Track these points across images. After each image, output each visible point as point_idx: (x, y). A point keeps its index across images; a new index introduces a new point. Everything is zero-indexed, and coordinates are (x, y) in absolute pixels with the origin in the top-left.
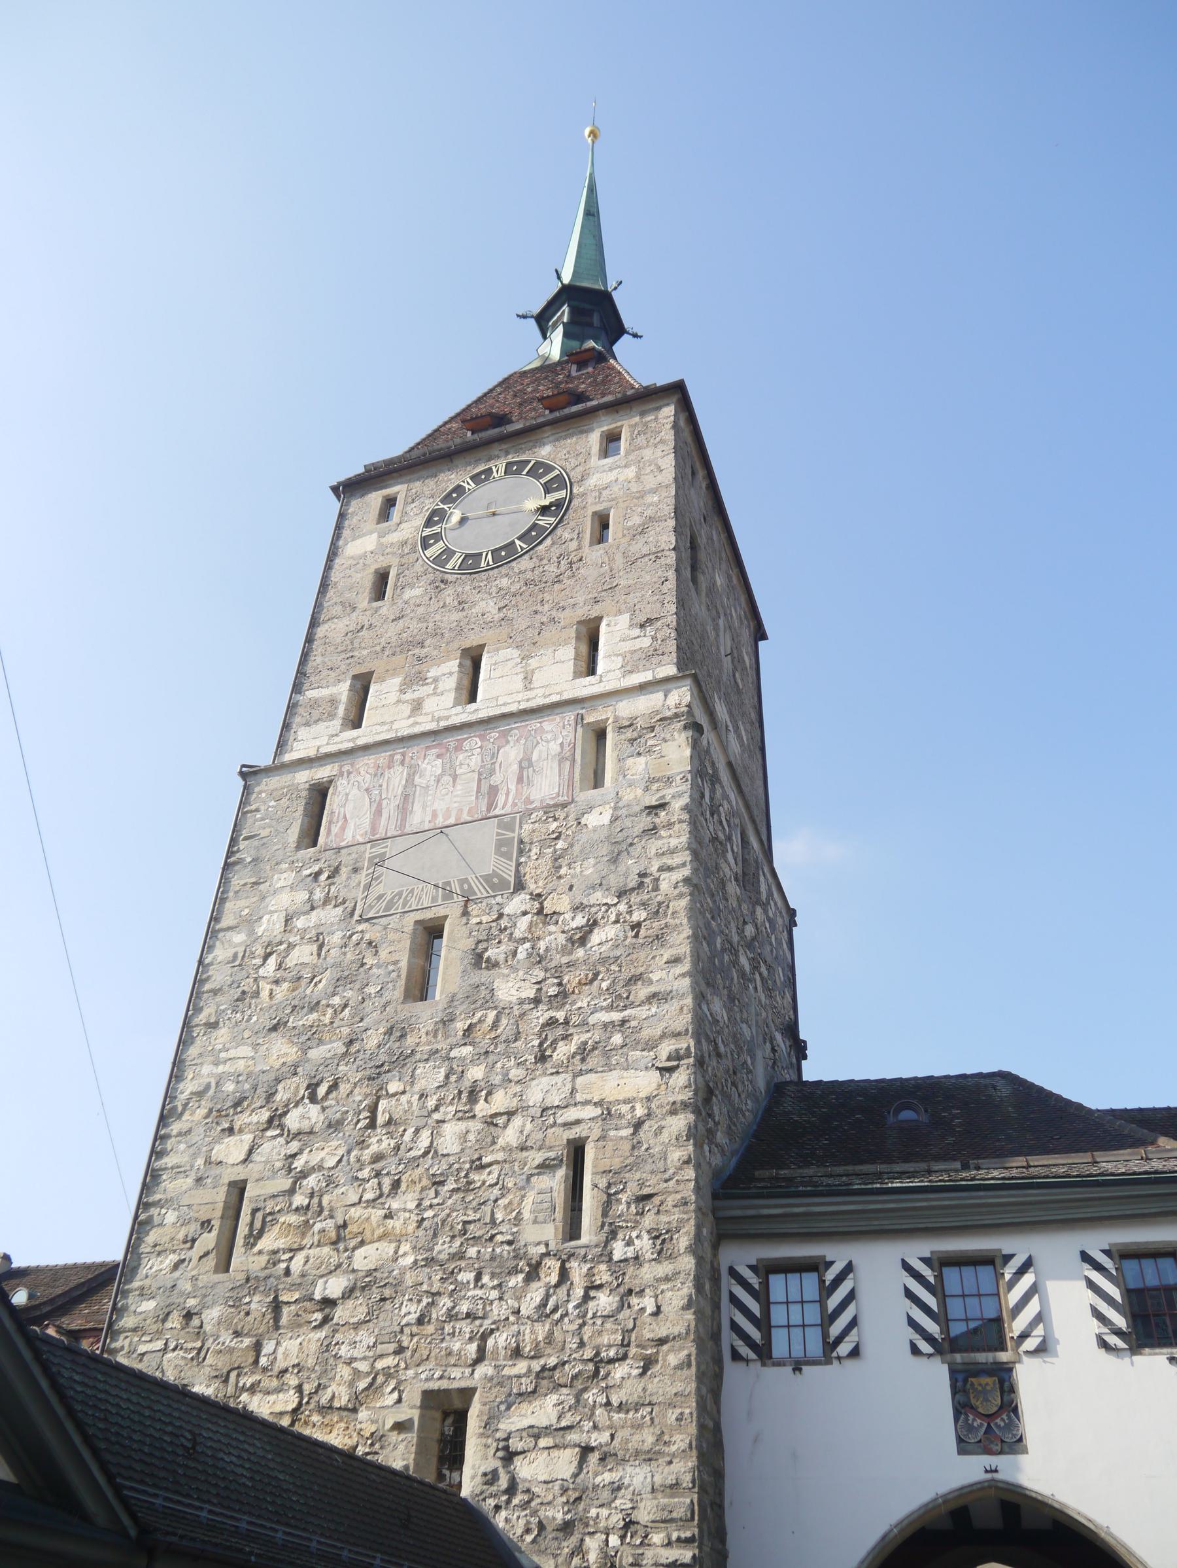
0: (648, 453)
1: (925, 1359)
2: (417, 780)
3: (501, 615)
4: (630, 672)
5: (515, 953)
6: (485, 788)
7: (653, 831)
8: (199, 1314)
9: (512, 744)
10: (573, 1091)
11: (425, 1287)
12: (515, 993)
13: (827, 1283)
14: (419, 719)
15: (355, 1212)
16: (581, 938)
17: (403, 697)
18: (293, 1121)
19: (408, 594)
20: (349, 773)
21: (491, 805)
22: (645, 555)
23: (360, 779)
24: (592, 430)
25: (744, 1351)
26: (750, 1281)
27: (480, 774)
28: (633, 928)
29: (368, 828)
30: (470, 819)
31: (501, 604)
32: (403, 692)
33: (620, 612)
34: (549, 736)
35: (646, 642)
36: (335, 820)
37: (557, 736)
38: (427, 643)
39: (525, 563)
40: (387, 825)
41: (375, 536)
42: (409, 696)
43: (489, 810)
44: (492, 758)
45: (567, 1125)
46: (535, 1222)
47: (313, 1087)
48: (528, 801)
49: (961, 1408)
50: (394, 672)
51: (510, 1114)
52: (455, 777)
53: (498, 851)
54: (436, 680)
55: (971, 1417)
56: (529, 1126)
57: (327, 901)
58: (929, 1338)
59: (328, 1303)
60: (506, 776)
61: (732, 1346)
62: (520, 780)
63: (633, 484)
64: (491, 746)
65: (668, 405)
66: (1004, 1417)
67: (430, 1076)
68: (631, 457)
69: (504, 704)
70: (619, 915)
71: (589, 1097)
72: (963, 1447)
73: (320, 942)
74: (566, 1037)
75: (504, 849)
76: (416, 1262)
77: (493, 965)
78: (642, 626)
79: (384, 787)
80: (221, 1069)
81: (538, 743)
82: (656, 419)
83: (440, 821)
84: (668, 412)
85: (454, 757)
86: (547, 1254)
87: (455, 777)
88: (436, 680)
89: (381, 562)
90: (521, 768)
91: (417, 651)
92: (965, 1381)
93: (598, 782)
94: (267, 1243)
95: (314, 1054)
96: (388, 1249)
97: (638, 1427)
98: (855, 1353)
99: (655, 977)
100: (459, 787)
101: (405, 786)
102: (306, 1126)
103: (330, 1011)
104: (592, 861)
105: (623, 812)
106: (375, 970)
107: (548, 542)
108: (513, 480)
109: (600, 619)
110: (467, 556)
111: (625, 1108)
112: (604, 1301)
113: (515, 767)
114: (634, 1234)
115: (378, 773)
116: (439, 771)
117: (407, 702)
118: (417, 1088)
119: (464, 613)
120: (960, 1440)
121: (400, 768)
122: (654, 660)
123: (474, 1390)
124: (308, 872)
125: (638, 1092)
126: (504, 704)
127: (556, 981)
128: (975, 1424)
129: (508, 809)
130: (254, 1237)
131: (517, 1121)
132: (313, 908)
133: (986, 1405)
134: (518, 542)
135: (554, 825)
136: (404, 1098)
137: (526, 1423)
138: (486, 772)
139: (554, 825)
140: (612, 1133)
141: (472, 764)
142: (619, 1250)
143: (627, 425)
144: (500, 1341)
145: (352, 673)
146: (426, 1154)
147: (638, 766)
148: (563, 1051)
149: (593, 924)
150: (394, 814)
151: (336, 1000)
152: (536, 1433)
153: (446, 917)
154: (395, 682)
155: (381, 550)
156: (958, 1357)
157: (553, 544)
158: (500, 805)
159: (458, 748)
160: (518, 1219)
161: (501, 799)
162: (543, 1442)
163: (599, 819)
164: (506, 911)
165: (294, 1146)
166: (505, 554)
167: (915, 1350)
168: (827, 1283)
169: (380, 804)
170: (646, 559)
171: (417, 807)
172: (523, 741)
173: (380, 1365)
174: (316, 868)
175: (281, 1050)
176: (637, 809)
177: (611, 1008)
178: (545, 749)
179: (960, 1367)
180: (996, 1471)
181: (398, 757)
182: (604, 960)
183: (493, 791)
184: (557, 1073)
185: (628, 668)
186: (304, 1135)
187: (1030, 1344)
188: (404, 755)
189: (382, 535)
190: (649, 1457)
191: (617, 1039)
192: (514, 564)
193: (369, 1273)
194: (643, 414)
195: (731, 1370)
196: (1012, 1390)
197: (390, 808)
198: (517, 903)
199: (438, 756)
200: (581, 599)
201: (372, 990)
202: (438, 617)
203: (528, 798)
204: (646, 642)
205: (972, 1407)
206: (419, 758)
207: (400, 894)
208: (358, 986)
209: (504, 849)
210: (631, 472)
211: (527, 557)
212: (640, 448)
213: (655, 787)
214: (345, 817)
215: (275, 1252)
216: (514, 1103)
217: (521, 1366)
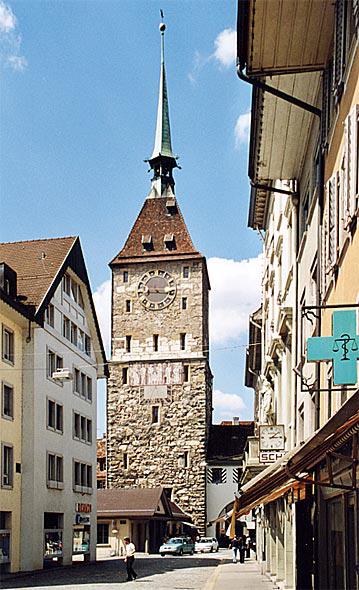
16: (186, 414)
18: (134, 443)
35: (195, 344)
37: (178, 367)
47: (137, 437)
59: (147, 475)
60: (168, 375)
89: (128, 298)
93: (187, 380)
94: (134, 464)
112: (192, 476)
125: (196, 444)
138: (164, 374)
142: (194, 469)
144: (176, 481)
148: (183, 436)
197: (143, 378)
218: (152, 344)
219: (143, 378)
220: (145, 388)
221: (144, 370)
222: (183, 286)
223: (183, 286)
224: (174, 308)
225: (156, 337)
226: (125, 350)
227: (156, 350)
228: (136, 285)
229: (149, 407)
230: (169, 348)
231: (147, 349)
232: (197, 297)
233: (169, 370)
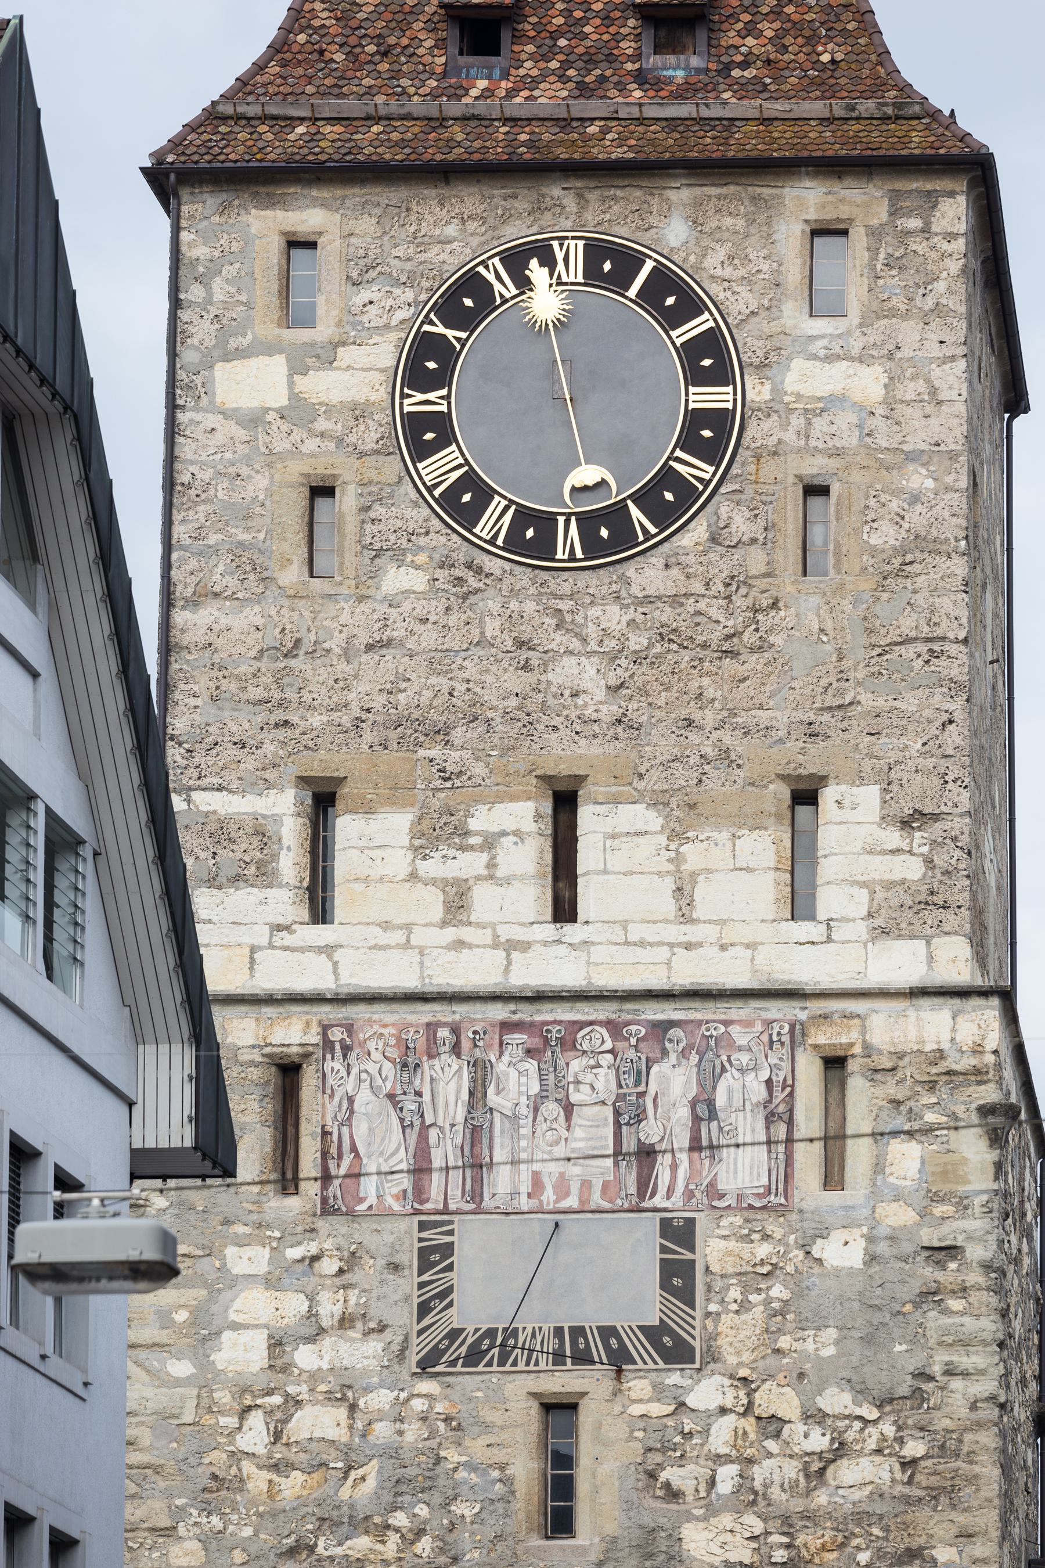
0: (909, 332)
4: (885, 932)
5: (712, 1483)
7: (931, 1296)
9: (673, 1057)
12: (719, 1551)
14: (467, 934)
16: (817, 1470)
17: (423, 866)
20: (346, 1049)
21: (645, 1185)
22: (907, 641)
27: (617, 1113)
28: (904, 1465)
30: (607, 1206)
32: (420, 852)
33: (860, 779)
34: (745, 1058)
35: (913, 869)
36: (334, 1150)
38: (458, 735)
39: (648, 575)
41: (278, 364)
42: (431, 867)
43: (641, 1194)
44: (637, 1083)
48: (713, 1192)
50: (396, 794)
52: (569, 1109)
53: (665, 1285)
54: (490, 842)
57: (345, 1322)
60: (668, 1123)
63: (878, 422)
64: (631, 1054)
69: (642, 944)
70: (883, 1438)
73: (345, 1394)
75: (677, 1282)
77: (673, 1494)
78: (906, 824)
79: (427, 1097)
81: (723, 1070)
82: (926, 230)
85: (561, 1062)
87: (569, 1109)
88: (490, 842)
89: (316, 457)
90: (696, 1119)
100: (578, 1133)
101: (471, 1107)
103: (394, 1538)
104: (832, 1333)
105: (882, 1248)
106: (462, 1474)
109: (822, 780)
113: (683, 1113)
116: (535, 1089)
117: (433, 882)
119: (531, 678)
122: (932, 916)
124: (294, 1253)
126: (642, 944)
127: (785, 1540)
132: (321, 1331)
134: (635, 512)
135: (763, 1250)
138: (628, 1112)
139: (763, 1250)
141: (599, 1085)
145: (293, 770)
147: (907, 1158)
149: (840, 1450)
151: (400, 1519)
153: (583, 1394)
154: (397, 824)
155: (299, 412)
158: (662, 1189)
159: (568, 1043)
163: (844, 1252)
164: (691, 1401)
172: (694, 1058)
174: (313, 1249)
176: (908, 1248)
178: (737, 1086)
182: (860, 1517)
183: (647, 1154)
185: (879, 922)
189: (297, 369)
197: (445, 1151)
198: (707, 1393)
200: (780, 718)
201: (463, 1509)
202: (472, 670)
203: (712, 1184)
204: (913, 869)
206: (487, 1048)
207: (491, 1333)
208: (437, 1499)
209: (677, 1282)
210: (868, 383)
212: (893, 313)
213: (939, 1210)
214: (354, 1149)
218: (528, 857)
219: (445, 1151)
220: (473, 1242)
221: (447, 1083)
222: (804, 378)
223: (804, 378)
224: (721, 566)
226: (284, 902)
227: (564, 910)
228: (385, 353)
229: (508, 1400)
230: (675, 901)
231: (484, 900)
232: (919, 479)
233: (674, 1081)
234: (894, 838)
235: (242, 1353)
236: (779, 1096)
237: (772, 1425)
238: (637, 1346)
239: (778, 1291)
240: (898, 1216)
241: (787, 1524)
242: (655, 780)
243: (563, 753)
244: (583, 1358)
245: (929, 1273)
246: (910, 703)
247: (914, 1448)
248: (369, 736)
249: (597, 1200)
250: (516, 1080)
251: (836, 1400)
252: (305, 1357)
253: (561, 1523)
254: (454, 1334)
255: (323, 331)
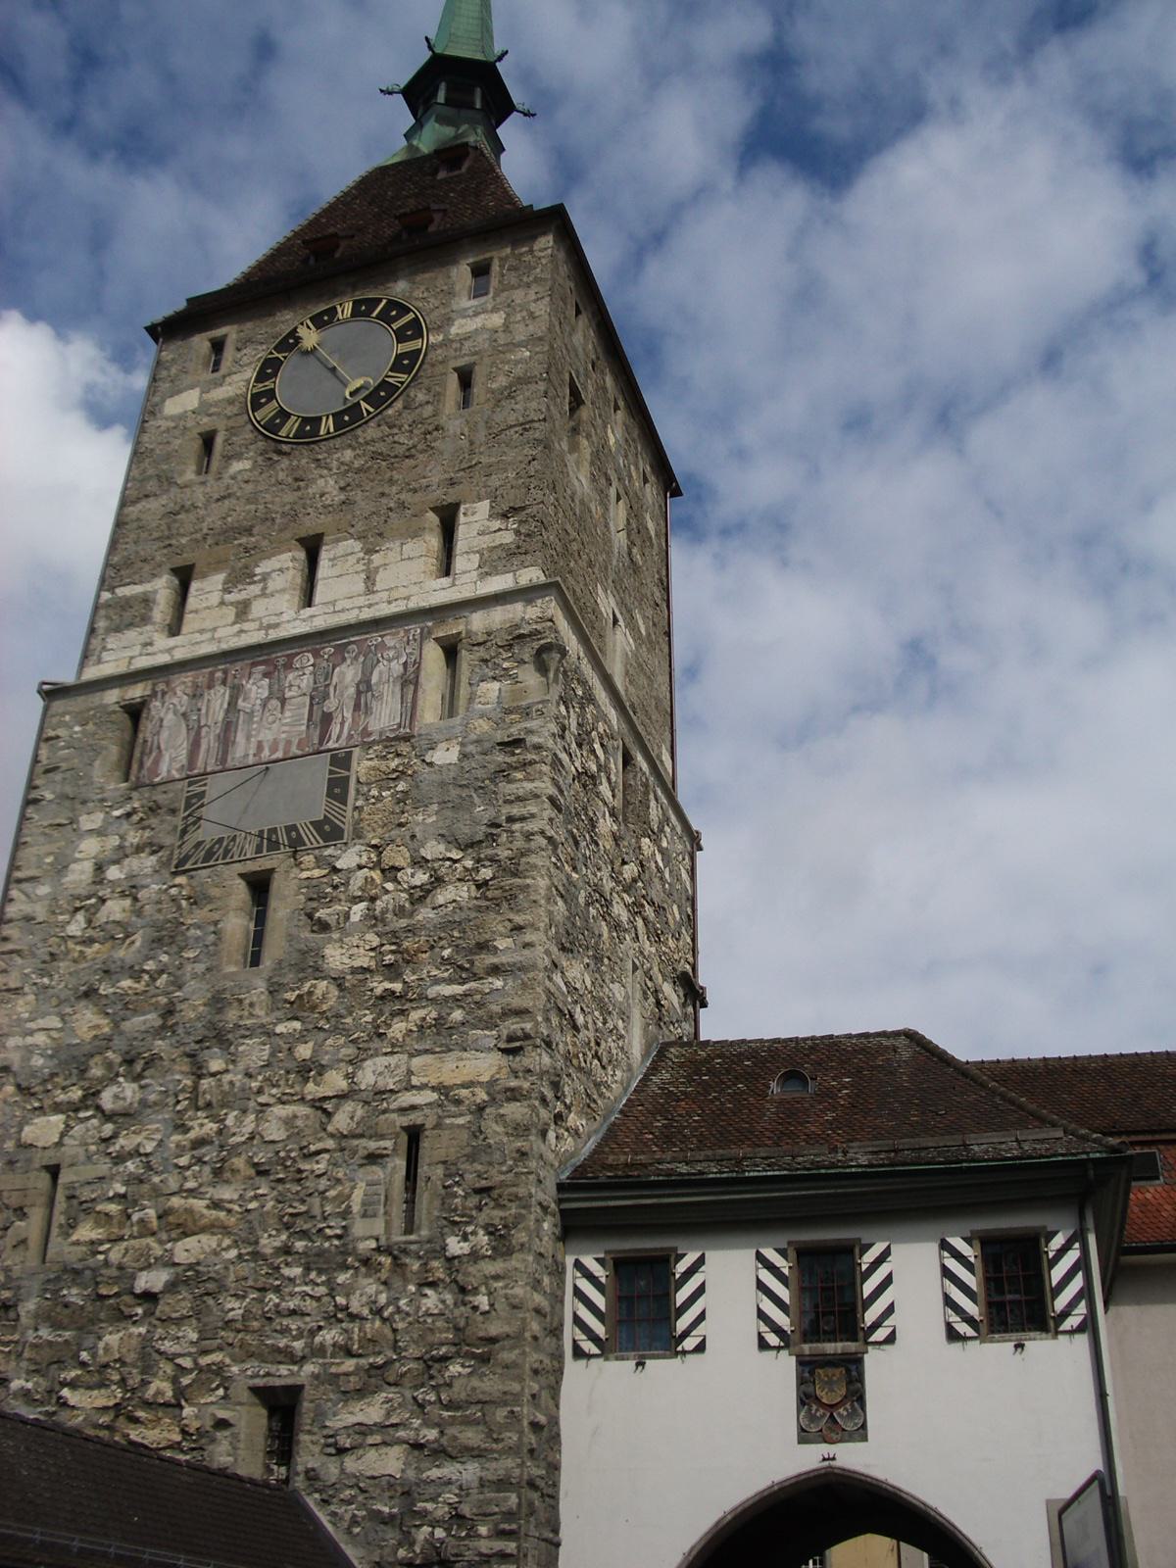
0: (518, 295)
1: (774, 1353)
2: (241, 703)
3: (342, 497)
4: (487, 574)
6: (317, 717)
8: (15, 1306)
9: (349, 661)
10: (410, 1073)
11: (250, 1283)
12: (347, 961)
13: (677, 1276)
14: (246, 626)
15: (176, 1202)
16: (421, 896)
17: (229, 597)
18: (107, 1100)
19: (237, 466)
20: (164, 693)
21: (324, 736)
22: (511, 427)
23: (175, 701)
24: (455, 262)
25: (589, 1346)
26: (596, 1274)
27: (312, 698)
28: (478, 887)
29: (185, 762)
30: (299, 753)
31: (342, 484)
32: (227, 591)
33: (480, 499)
34: (391, 653)
36: (148, 751)
38: (255, 531)
39: (371, 432)
40: (206, 760)
43: (321, 743)
44: (326, 680)
45: (403, 1110)
46: (364, 1215)
47: (129, 1062)
48: (366, 733)
49: (805, 1399)
50: (217, 565)
51: (342, 1097)
52: (283, 701)
55: (814, 1407)
56: (360, 1112)
58: (777, 1330)
59: (149, 1297)
61: (574, 1341)
62: (357, 707)
64: (325, 664)
65: (544, 233)
66: (848, 1406)
67: (254, 1052)
68: (498, 300)
69: (342, 611)
71: (425, 1080)
72: (804, 1436)
74: (403, 1012)
75: (337, 791)
76: (240, 1256)
77: (324, 927)
79: (203, 711)
80: (29, 1040)
81: (378, 661)
82: (531, 251)
83: (266, 754)
84: (546, 243)
85: (282, 677)
86: (378, 1249)
87: (283, 701)
88: (265, 578)
89: (207, 423)
90: (359, 693)
91: (243, 540)
92: (812, 1373)
94: (86, 1232)
95: (126, 1026)
96: (209, 1241)
97: (468, 1422)
98: (700, 1348)
99: (502, 944)
100: (288, 714)
101: (227, 711)
102: (120, 1105)
105: (471, 748)
107: (399, 405)
108: (361, 326)
110: (306, 421)
111: (464, 1093)
113: (352, 690)
114: (470, 1229)
115: (196, 695)
116: (266, 694)
117: (232, 604)
118: (241, 1066)
119: (299, 494)
120: (802, 1430)
121: (221, 689)
123: (301, 1388)
126: (342, 611)
128: (818, 1414)
129: (342, 742)
130: (72, 1225)
131: (348, 1106)
133: (832, 1392)
134: (363, 405)
136: (227, 1078)
137: (352, 1420)
138: (318, 696)
140: (448, 1121)
141: (303, 685)
142: (455, 1246)
143: (500, 256)
145: (169, 566)
146: (252, 1138)
148: (398, 1029)
149: (438, 881)
150: (214, 744)
151: (150, 966)
152: (363, 1429)
154: (218, 579)
155: (204, 408)
156: (806, 1348)
157: (405, 408)
158: (334, 737)
160: (346, 1214)
161: (335, 729)
162: (370, 1440)
164: (339, 865)
165: (108, 1129)
166: (349, 418)
167: (763, 1345)
168: (677, 1276)
169: (198, 733)
170: (512, 431)
171: (240, 738)
172: (361, 659)
173: (204, 1361)
175: (88, 1022)
177: (450, 981)
178: (385, 669)
179: (808, 1359)
180: (834, 1459)
181: (219, 675)
183: (327, 719)
184: (392, 1053)
185: (486, 569)
186: (123, 1117)
187: (880, 1335)
188: (225, 672)
190: (478, 1454)
191: (457, 1015)
192: (359, 432)
193: (191, 1267)
194: (515, 244)
195: (572, 1368)
196: (861, 1379)
197: (209, 741)
198: (348, 859)
199: (266, 675)
203: (365, 729)
204: (508, 538)
205: (817, 1398)
206: (243, 676)
207: (221, 840)
209: (337, 791)
210: (497, 320)
211: (372, 424)
214: (159, 747)
215: (92, 1242)
216: (343, 1084)
217: (349, 1365)
220: (214, 787)
225: (312, 548)
234: (497, 524)
235: (80, 874)
236: (411, 669)
237: (391, 872)
238: (311, 837)
239: (401, 786)
240: (483, 726)
241: (394, 937)
242: (360, 527)
243: (310, 525)
244: (274, 845)
245: (500, 758)
246: (511, 455)
247: (486, 873)
248: (210, 541)
249: (294, 750)
250: (257, 688)
251: (432, 849)
252: (114, 873)
253: (255, 960)
254: (199, 844)
255: (223, 370)
